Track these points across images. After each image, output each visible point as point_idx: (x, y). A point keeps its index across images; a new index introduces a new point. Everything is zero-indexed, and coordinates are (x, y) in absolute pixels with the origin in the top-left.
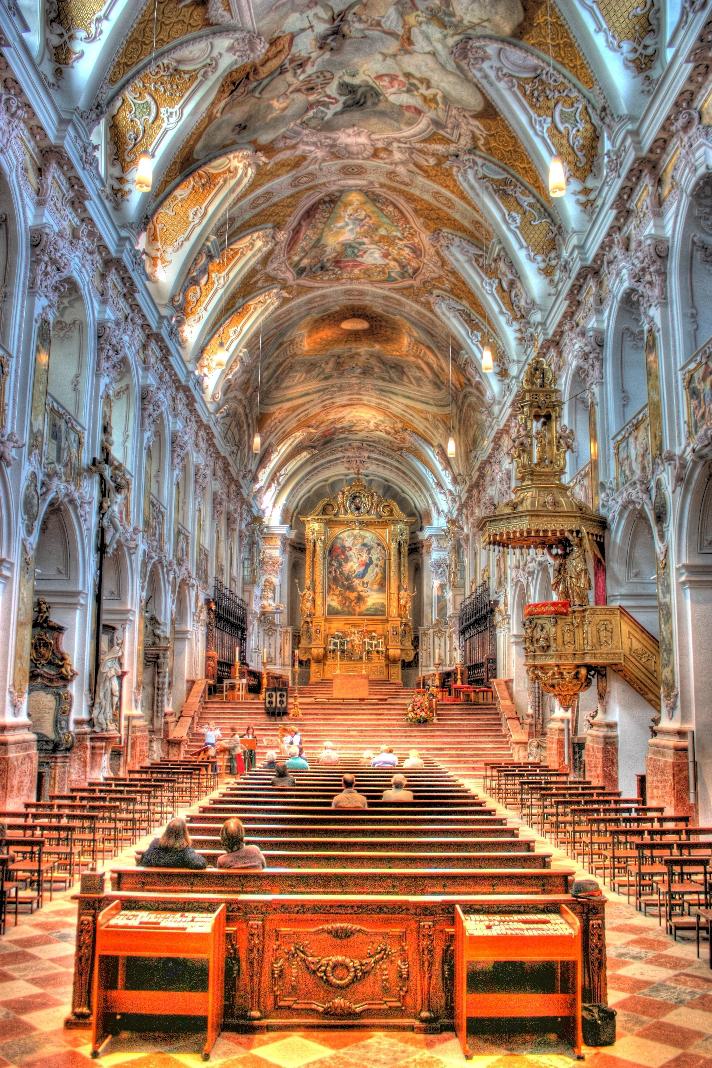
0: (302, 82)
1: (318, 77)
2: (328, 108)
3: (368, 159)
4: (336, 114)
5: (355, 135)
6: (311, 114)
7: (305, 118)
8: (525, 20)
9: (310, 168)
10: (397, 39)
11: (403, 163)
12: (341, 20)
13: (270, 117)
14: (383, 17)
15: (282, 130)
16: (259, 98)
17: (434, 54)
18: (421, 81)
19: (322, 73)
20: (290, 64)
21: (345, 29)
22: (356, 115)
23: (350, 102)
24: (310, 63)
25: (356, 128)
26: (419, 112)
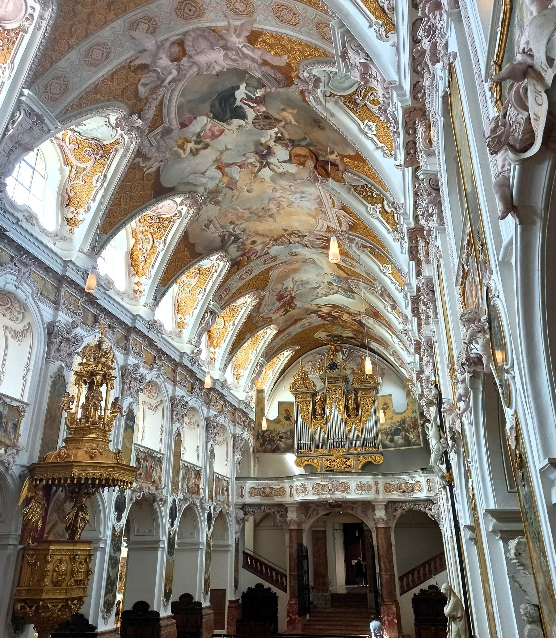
0: (275, 126)
1: (264, 126)
2: (246, 94)
3: (186, 34)
4: (238, 88)
5: (211, 64)
6: (259, 93)
7: (263, 90)
8: (189, 242)
9: (238, 23)
10: (226, 164)
11: (155, 56)
12: (262, 163)
13: (295, 111)
14: (240, 172)
15: (281, 90)
16: (305, 134)
17: (203, 174)
18: (198, 150)
19: (263, 129)
20: (287, 144)
21: (258, 158)
22: (220, 88)
23: (232, 100)
24: (274, 138)
25: (214, 72)
26: (183, 125)
